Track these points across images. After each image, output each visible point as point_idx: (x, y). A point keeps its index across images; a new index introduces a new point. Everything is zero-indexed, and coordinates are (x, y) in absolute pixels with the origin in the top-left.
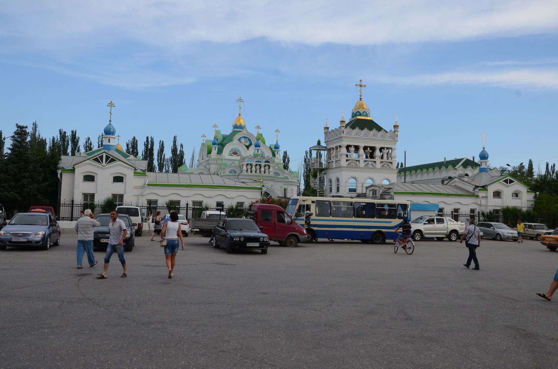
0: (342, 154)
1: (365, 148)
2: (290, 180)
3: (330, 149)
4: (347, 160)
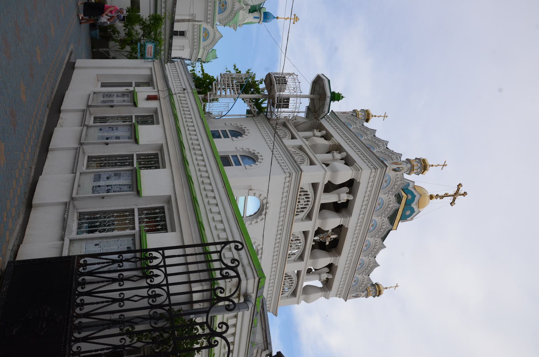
0: (335, 171)
1: (340, 230)
2: (202, 44)
3: (321, 128)
4: (315, 186)
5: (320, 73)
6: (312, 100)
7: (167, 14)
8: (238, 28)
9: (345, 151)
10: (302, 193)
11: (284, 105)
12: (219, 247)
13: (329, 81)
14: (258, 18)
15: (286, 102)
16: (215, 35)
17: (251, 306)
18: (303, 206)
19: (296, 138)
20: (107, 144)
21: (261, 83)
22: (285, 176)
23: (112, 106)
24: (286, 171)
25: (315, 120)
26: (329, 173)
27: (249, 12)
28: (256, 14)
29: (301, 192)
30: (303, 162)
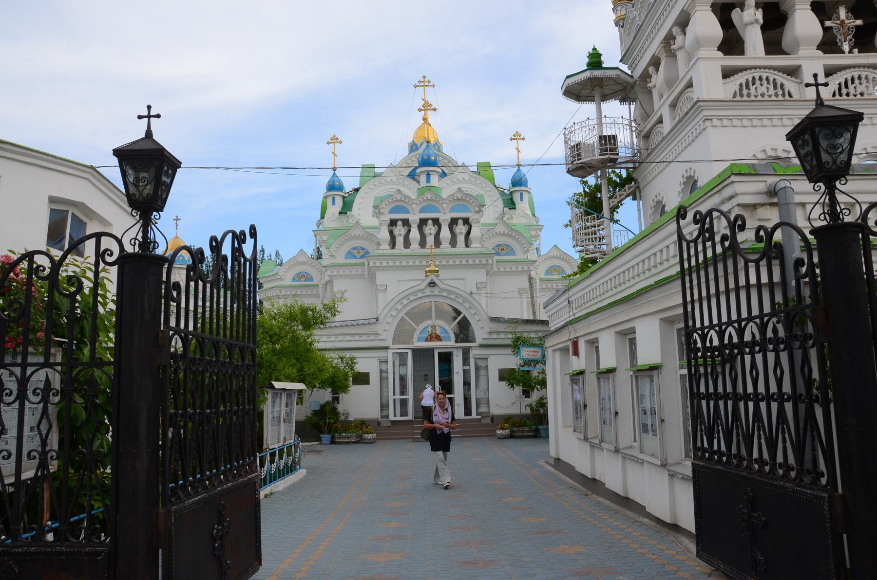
0: (698, 44)
3: (646, 76)
4: (728, 73)
5: (561, 93)
6: (605, 98)
7: (510, 329)
8: (540, 223)
9: (670, 30)
10: (745, 92)
11: (610, 143)
12: (684, 244)
13: (568, 77)
14: (521, 194)
15: (605, 140)
16: (554, 257)
17: (782, 185)
18: (771, 87)
19: (661, 116)
20: (617, 413)
21: (586, 183)
22: (710, 130)
23: (585, 406)
24: (702, 127)
25: (637, 88)
26: (702, 53)
27: (515, 208)
28: (516, 197)
29: (742, 95)
30: (689, 99)
